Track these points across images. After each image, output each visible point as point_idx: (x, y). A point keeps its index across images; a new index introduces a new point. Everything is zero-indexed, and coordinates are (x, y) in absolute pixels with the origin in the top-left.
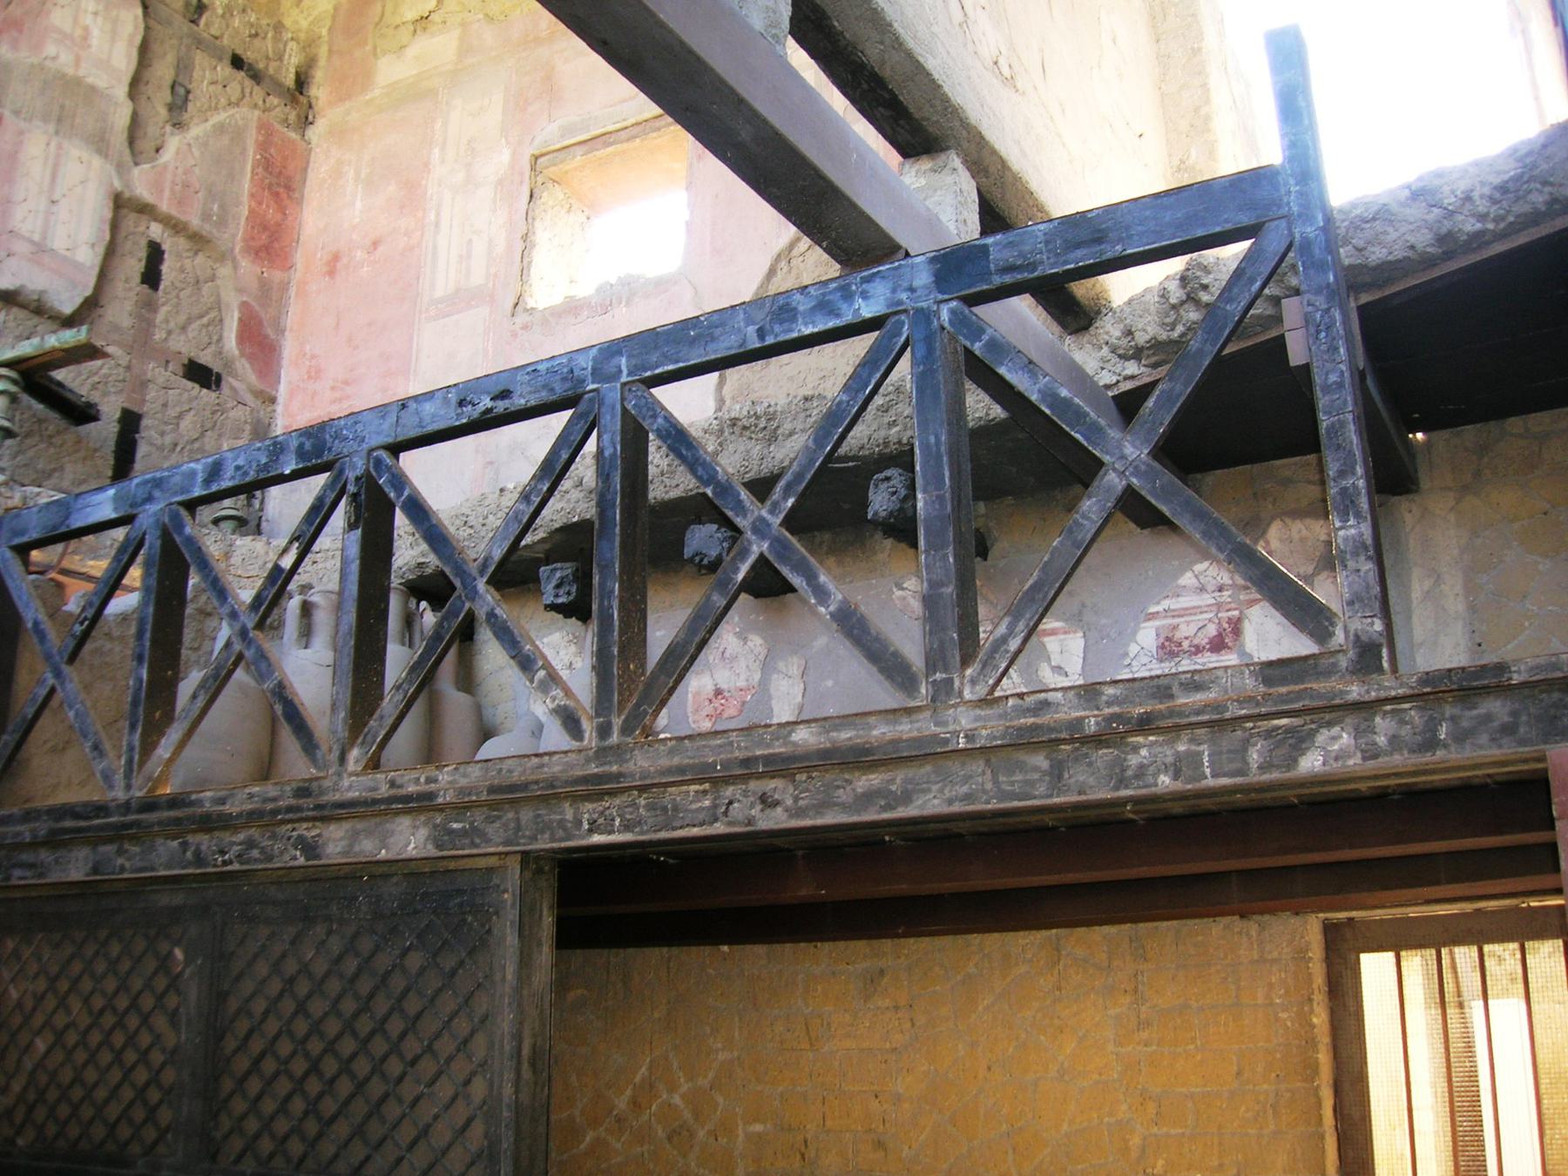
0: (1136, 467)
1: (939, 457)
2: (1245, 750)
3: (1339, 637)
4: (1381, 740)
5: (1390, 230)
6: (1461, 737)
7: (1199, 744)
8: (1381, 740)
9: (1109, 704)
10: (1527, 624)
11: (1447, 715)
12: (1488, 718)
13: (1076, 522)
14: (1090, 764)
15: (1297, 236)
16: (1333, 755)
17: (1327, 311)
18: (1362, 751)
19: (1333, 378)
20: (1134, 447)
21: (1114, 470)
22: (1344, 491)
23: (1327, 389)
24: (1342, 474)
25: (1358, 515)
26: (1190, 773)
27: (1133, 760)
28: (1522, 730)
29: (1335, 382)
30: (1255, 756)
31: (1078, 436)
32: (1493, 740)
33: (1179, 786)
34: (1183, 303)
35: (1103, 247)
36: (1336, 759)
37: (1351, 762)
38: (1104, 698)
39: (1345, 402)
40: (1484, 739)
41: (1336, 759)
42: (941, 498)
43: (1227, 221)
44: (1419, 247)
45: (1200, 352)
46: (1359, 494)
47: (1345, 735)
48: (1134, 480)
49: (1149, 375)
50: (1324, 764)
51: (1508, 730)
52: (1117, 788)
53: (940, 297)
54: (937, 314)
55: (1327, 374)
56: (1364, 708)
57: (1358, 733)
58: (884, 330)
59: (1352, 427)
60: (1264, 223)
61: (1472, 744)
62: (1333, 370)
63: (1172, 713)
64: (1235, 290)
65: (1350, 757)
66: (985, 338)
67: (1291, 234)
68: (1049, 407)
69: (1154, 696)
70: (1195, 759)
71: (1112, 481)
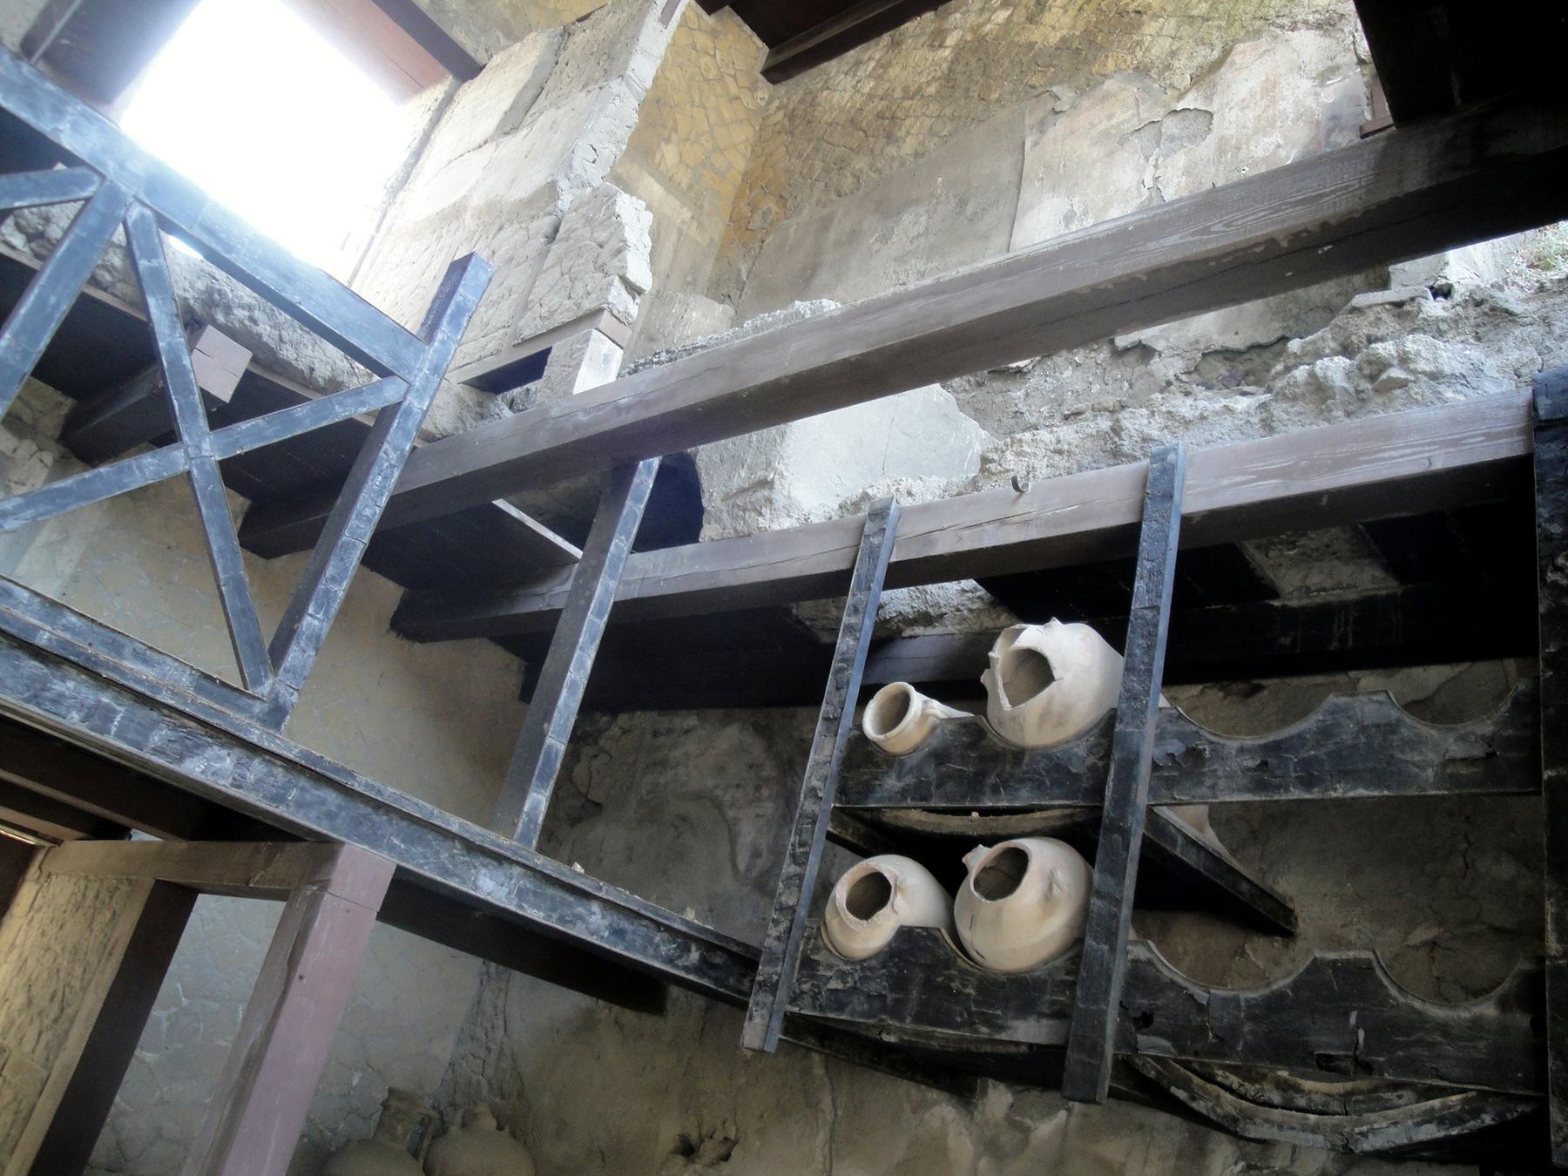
0: (203, 464)
1: (49, 319)
2: (151, 730)
3: (264, 689)
4: (251, 777)
5: (310, 347)
6: (300, 805)
7: (120, 705)
8: (251, 777)
9: (65, 628)
10: (105, 614)
11: (300, 785)
12: (323, 802)
13: (130, 467)
14: (17, 668)
15: (405, 404)
16: (213, 769)
17: (392, 466)
18: (234, 779)
19: (368, 512)
20: (211, 445)
21: (186, 452)
22: (327, 591)
23: (360, 515)
24: (333, 579)
25: (326, 613)
26: (98, 723)
27: (58, 686)
28: (338, 821)
29: (367, 516)
30: (156, 738)
31: (175, 402)
32: (318, 817)
33: (83, 728)
34: (119, 246)
35: (288, 286)
36: (214, 774)
37: (222, 782)
38: (64, 621)
39: (365, 534)
40: (313, 814)
41: (214, 774)
42: (25, 354)
43: (374, 350)
44: (317, 373)
45: (299, 422)
46: (335, 601)
47: (228, 760)
48: (195, 472)
49: (30, 260)
50: (202, 772)
51: (331, 816)
52: (28, 701)
53: (142, 196)
54: (128, 207)
55: (366, 506)
56: (254, 749)
57: (238, 764)
58: (70, 170)
59: (358, 553)
60: (393, 374)
61: (305, 814)
62: (370, 508)
63: (116, 669)
64: (349, 401)
65: (223, 777)
66: (155, 263)
67: (405, 397)
68: (169, 363)
69: (106, 645)
70: (108, 715)
71: (175, 459)
